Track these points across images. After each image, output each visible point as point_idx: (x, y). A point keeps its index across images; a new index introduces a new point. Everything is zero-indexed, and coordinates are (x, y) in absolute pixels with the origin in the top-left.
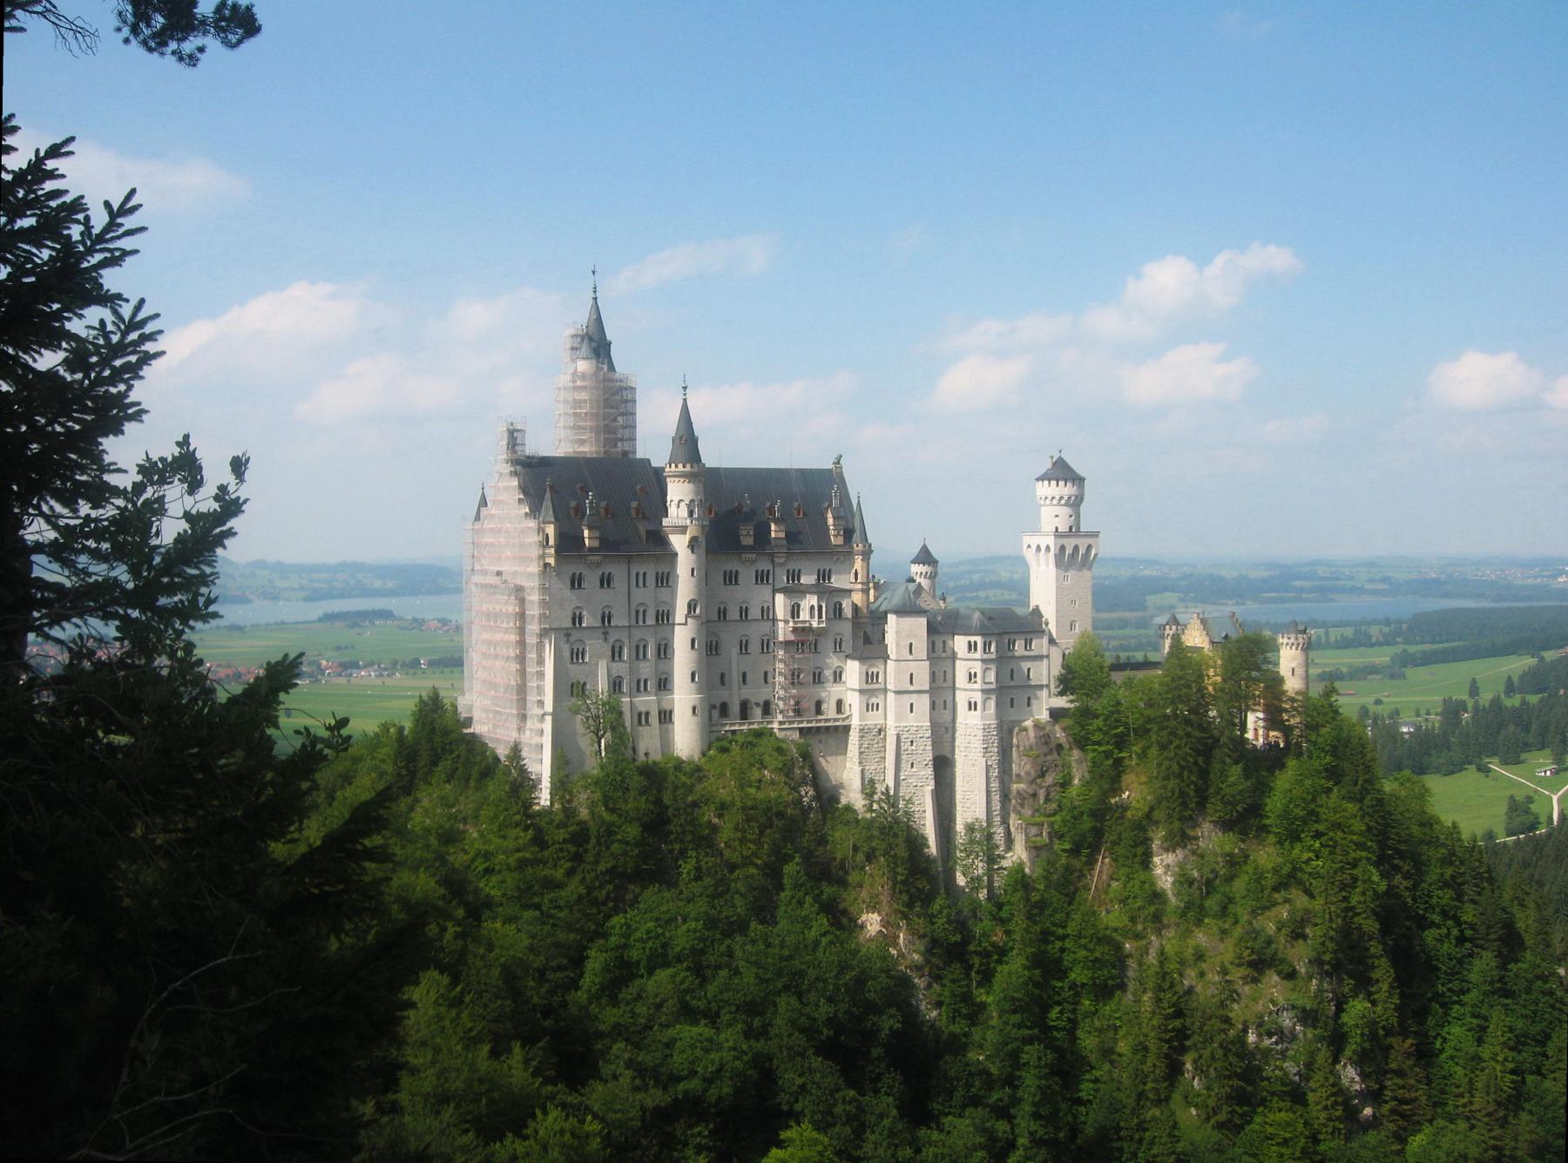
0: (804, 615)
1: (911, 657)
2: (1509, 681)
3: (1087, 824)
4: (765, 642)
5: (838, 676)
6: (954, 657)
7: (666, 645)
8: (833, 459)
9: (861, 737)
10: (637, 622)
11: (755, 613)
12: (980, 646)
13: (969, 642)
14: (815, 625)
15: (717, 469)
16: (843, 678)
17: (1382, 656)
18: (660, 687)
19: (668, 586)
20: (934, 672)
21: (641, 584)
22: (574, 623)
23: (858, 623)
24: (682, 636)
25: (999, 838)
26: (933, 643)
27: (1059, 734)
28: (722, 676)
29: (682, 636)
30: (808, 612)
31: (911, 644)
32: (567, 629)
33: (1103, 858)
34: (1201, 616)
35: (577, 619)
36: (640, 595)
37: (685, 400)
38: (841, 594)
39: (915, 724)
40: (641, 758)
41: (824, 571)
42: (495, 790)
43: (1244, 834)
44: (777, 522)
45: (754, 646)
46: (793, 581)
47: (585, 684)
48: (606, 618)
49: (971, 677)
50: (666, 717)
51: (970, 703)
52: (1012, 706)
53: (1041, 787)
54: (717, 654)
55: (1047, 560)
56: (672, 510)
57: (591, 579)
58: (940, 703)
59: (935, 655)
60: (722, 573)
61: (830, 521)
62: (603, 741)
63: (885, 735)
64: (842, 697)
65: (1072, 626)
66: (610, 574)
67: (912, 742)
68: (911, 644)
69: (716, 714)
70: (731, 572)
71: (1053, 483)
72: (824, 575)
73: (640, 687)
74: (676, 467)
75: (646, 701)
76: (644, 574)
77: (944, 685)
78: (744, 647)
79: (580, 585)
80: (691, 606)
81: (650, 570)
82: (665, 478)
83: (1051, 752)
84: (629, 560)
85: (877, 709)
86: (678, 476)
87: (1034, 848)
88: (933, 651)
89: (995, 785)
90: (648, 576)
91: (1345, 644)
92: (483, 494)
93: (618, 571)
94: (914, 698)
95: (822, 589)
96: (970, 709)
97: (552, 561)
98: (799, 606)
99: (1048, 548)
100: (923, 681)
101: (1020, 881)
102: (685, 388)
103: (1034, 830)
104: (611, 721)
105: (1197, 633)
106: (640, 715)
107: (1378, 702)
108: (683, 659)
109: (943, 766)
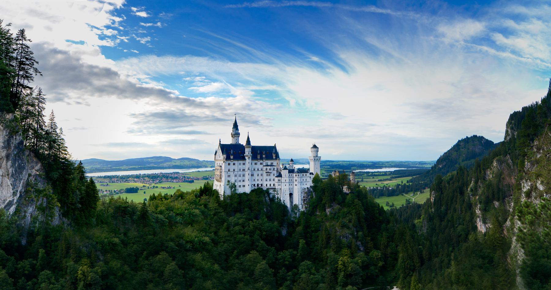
0: (268, 170)
2: (407, 181)
3: (316, 204)
5: (274, 180)
11: (260, 169)
14: (270, 171)
17: (389, 177)
24: (247, 173)
25: (300, 207)
27: (311, 190)
29: (247, 173)
35: (229, 170)
36: (240, 166)
40: (239, 192)
42: (214, 197)
43: (341, 206)
45: (260, 175)
48: (234, 170)
49: (296, 181)
50: (244, 186)
57: (232, 164)
58: (291, 184)
62: (233, 190)
69: (253, 186)
73: (240, 181)
75: (241, 184)
78: (258, 175)
80: (249, 169)
81: (242, 162)
84: (238, 160)
87: (306, 208)
89: (300, 198)
91: (383, 175)
94: (286, 184)
95: (272, 165)
97: (225, 161)
100: (288, 181)
101: (303, 213)
103: (306, 205)
104: (233, 186)
107: (387, 184)
108: (247, 177)
109: (291, 195)
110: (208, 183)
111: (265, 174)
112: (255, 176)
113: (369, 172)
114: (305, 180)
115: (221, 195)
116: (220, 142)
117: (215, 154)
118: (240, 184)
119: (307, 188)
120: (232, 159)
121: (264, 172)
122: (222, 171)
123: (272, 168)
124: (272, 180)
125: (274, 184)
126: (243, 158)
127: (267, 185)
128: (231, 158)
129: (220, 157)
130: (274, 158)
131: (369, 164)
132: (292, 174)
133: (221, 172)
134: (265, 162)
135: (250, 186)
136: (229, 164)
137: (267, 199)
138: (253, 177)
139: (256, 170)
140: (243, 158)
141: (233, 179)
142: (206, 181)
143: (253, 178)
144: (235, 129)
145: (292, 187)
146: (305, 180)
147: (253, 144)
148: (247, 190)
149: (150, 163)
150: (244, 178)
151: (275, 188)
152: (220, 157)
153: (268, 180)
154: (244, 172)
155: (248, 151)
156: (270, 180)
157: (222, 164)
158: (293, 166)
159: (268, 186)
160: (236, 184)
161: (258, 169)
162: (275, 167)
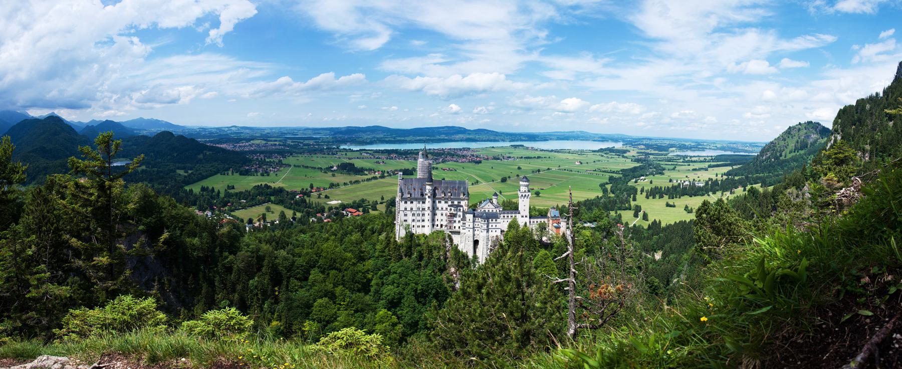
24: (428, 213)
45: (444, 215)
48: (412, 209)
78: (442, 215)
80: (429, 208)
91: (701, 162)
93: (414, 202)
108: (428, 217)
113: (687, 157)
114: (494, 227)
118: (418, 224)
131: (692, 144)
146: (494, 227)
149: (440, 133)
150: (423, 218)
154: (423, 212)
161: (442, 208)
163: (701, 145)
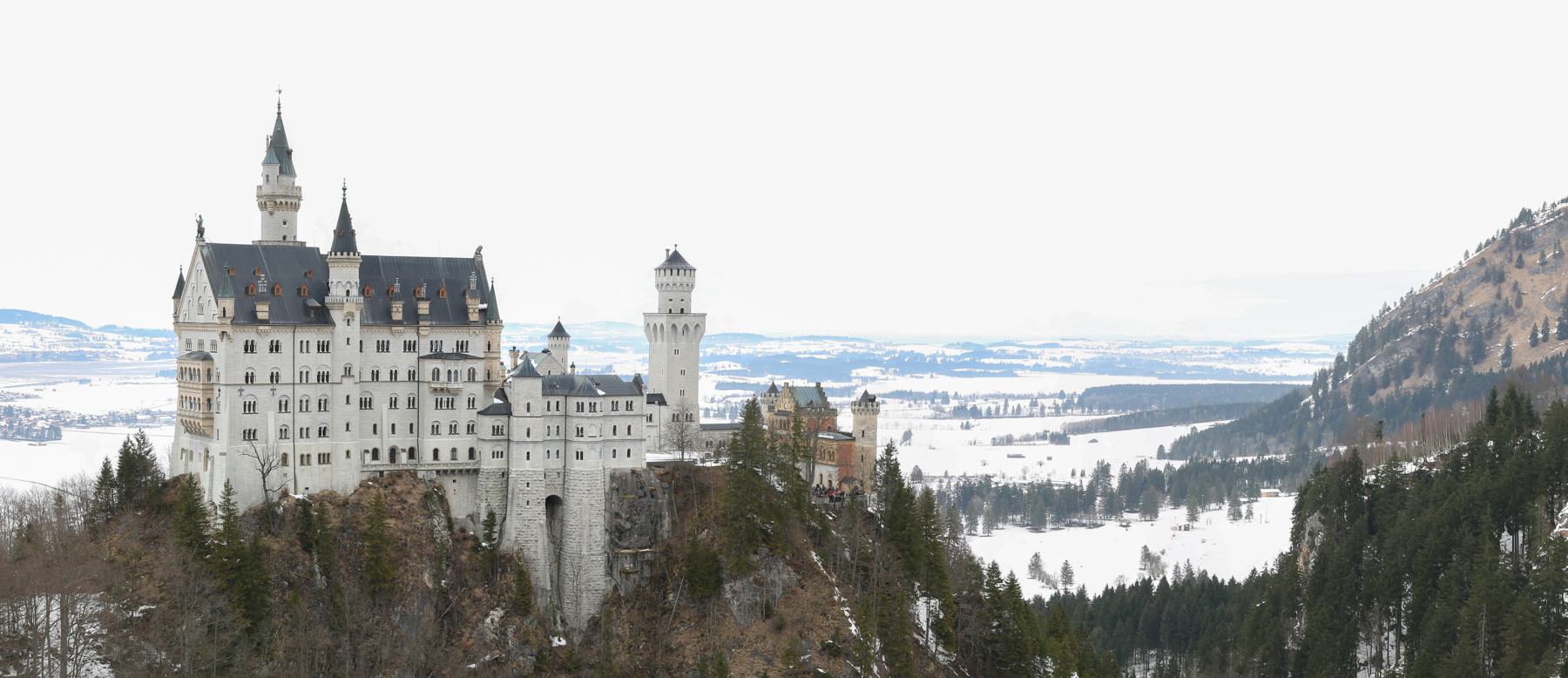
0: (443, 377)
1: (528, 414)
4: (412, 399)
6: (566, 416)
7: (325, 400)
8: (475, 251)
9: (487, 478)
10: (301, 381)
11: (402, 376)
12: (587, 407)
13: (578, 403)
15: (376, 258)
16: (475, 431)
18: (320, 435)
19: (328, 352)
20: (549, 427)
21: (304, 350)
22: (247, 381)
23: (491, 386)
26: (549, 403)
28: (375, 426)
30: (446, 375)
31: (528, 404)
32: (242, 385)
33: (684, 584)
34: (790, 385)
35: (249, 379)
37: (344, 199)
38: (475, 361)
39: (531, 469)
41: (462, 342)
44: (423, 299)
45: (402, 403)
46: (436, 350)
47: (255, 431)
48: (275, 378)
51: (577, 452)
52: (614, 457)
53: (635, 524)
54: (370, 408)
55: (662, 336)
56: (333, 290)
57: (262, 345)
59: (549, 413)
60: (376, 343)
61: (469, 301)
63: (508, 478)
64: (474, 446)
65: (682, 393)
66: (277, 341)
67: (528, 484)
68: (528, 404)
69: (368, 457)
70: (383, 341)
71: (668, 272)
72: (461, 346)
73: (304, 433)
74: (336, 254)
76: (308, 342)
77: (557, 438)
78: (393, 403)
79: (252, 351)
80: (348, 372)
81: (313, 336)
82: (327, 263)
83: (645, 495)
85: (502, 457)
86: (339, 262)
88: (549, 409)
90: (310, 344)
92: (181, 275)
94: (530, 448)
95: (461, 353)
96: (577, 458)
97: (229, 330)
98: (438, 370)
99: (662, 325)
100: (538, 433)
102: (344, 189)
105: (787, 400)
106: (302, 456)
108: (342, 413)
110: (142, 439)
111: (428, 401)
112: (382, 413)
114: (621, 433)
115: (213, 504)
116: (201, 231)
117: (179, 293)
118: (304, 446)
119: (633, 472)
120: (264, 322)
121: (425, 388)
122: (214, 380)
123: (463, 367)
124: (462, 429)
125: (472, 452)
126: (322, 317)
127: (436, 452)
128: (260, 316)
129: (201, 307)
130: (474, 317)
132: (561, 399)
133: (209, 388)
134: (427, 338)
135: (355, 456)
136: (249, 348)
137: (439, 522)
138: (368, 412)
139: (385, 376)
140: (322, 317)
141: (271, 421)
142: (131, 432)
143: (370, 416)
144: (277, 169)
145: (556, 464)
146: (621, 433)
147: (367, 245)
148: (345, 477)
150: (323, 418)
151: (476, 471)
152: (201, 307)
153: (444, 430)
154: (323, 390)
155: (344, 279)
156: (453, 430)
157: (214, 344)
158: (564, 360)
159: (445, 456)
160: (286, 446)
161: (394, 375)
162: (480, 367)
163: (995, 355)
